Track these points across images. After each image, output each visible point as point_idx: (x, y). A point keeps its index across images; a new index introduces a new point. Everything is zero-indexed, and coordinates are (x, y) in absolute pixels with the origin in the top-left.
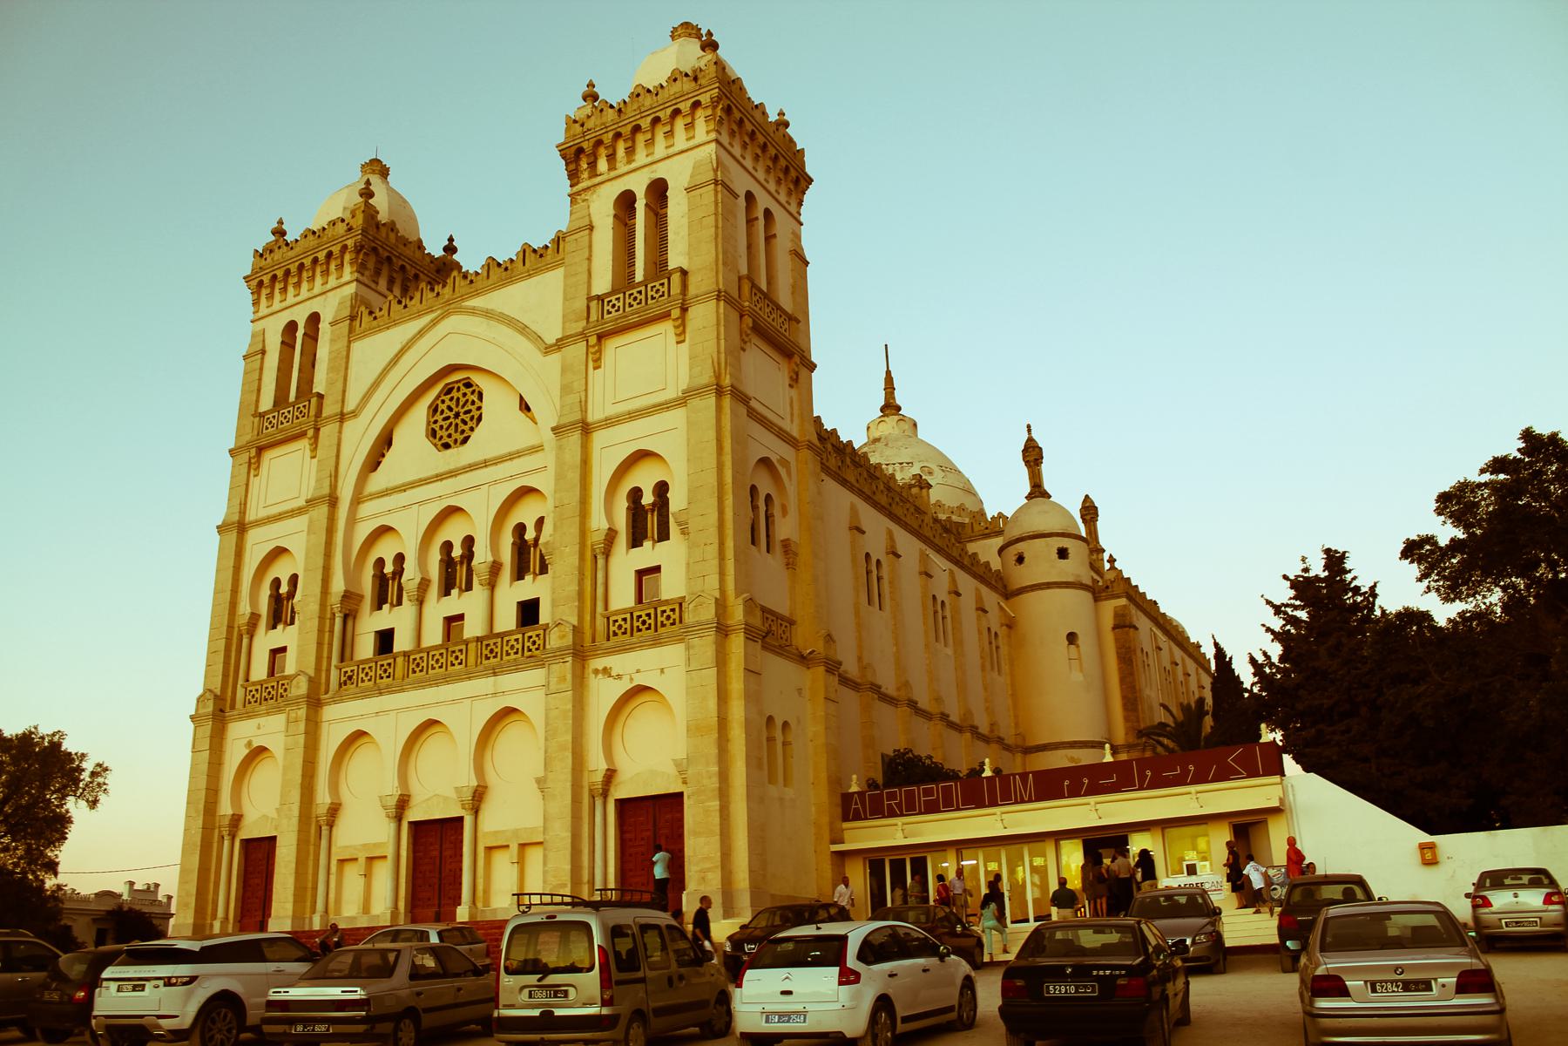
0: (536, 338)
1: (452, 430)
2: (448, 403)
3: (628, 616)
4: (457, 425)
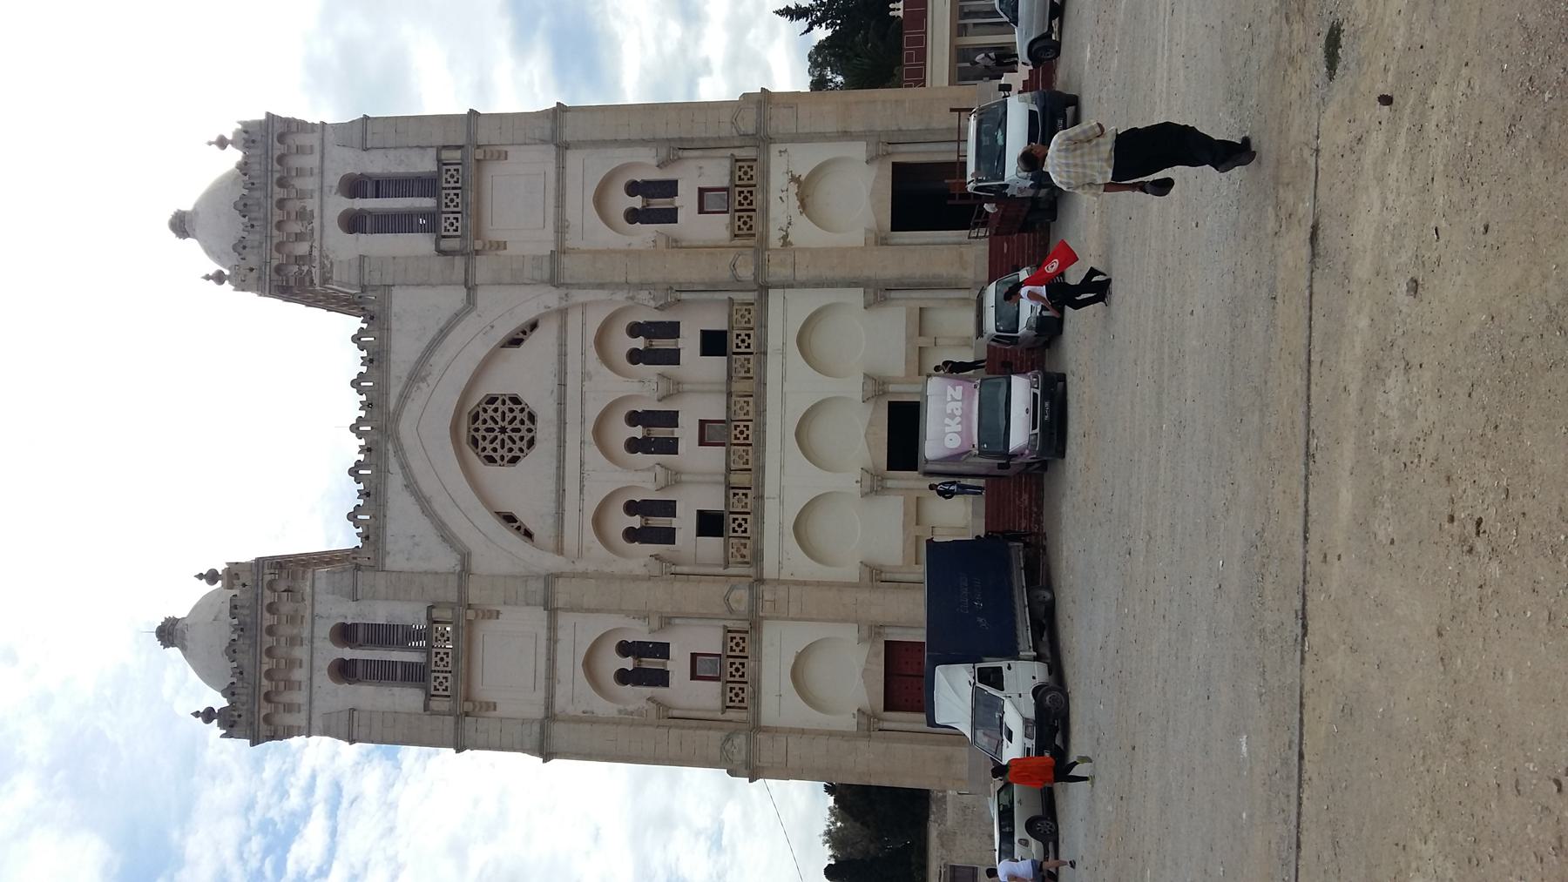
0: (457, 318)
1: (516, 436)
2: (490, 412)
3: (737, 214)
4: (510, 438)
